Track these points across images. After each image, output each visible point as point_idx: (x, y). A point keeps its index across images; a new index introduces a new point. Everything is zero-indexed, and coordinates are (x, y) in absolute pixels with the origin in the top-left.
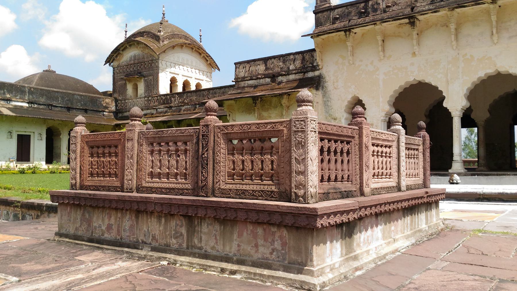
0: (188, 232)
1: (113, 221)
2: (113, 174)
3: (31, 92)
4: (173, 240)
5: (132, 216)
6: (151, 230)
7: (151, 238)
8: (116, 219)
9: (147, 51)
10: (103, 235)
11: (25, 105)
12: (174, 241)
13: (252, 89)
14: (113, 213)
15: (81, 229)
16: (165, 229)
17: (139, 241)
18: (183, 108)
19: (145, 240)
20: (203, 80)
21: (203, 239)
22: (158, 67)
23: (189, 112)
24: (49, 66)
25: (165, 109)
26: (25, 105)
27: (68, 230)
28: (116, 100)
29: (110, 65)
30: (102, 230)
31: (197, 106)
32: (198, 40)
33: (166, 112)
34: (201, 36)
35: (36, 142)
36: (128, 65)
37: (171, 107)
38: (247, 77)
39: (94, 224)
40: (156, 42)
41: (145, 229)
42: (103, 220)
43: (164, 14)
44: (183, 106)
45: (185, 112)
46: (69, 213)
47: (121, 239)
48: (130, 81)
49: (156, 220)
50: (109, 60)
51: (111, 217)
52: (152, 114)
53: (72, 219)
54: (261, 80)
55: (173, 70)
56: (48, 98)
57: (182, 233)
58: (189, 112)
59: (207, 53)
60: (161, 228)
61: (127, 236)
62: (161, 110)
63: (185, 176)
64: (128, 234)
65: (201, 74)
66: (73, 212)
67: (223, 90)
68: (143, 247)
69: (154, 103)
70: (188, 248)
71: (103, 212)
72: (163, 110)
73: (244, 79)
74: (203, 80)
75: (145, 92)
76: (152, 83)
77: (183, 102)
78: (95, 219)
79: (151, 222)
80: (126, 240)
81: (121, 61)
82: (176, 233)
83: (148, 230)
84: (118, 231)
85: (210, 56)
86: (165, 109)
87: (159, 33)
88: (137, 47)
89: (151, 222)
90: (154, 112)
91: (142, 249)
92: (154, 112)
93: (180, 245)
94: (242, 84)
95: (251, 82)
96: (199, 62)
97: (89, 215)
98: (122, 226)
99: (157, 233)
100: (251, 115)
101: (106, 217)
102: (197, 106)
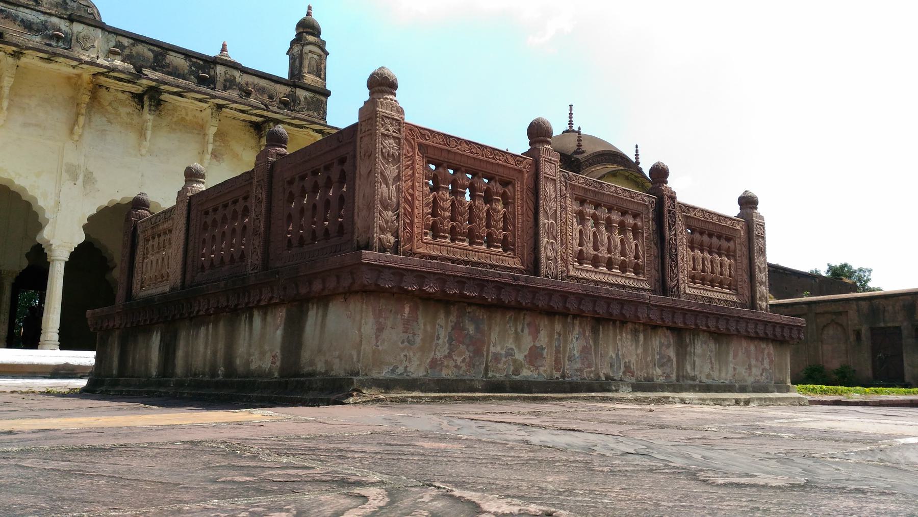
0: (678, 355)
1: (543, 339)
2: (498, 241)
4: (658, 369)
5: (584, 331)
6: (623, 355)
7: (623, 369)
8: (551, 337)
10: (516, 372)
12: (659, 371)
14: (544, 323)
15: (452, 363)
16: (645, 351)
17: (599, 377)
19: (611, 375)
21: (697, 363)
27: (401, 370)
30: (515, 361)
39: (492, 349)
41: (612, 353)
42: (517, 338)
46: (407, 323)
47: (563, 377)
49: (629, 337)
51: (538, 331)
53: (418, 340)
57: (669, 357)
60: (640, 351)
61: (577, 370)
63: (637, 270)
64: (578, 366)
66: (421, 321)
68: (619, 386)
70: (678, 380)
71: (516, 320)
78: (494, 336)
79: (621, 340)
80: (575, 378)
82: (662, 357)
83: (617, 355)
84: (557, 361)
89: (621, 340)
91: (617, 391)
93: (668, 377)
97: (477, 329)
98: (565, 351)
99: (633, 359)
101: (526, 331)
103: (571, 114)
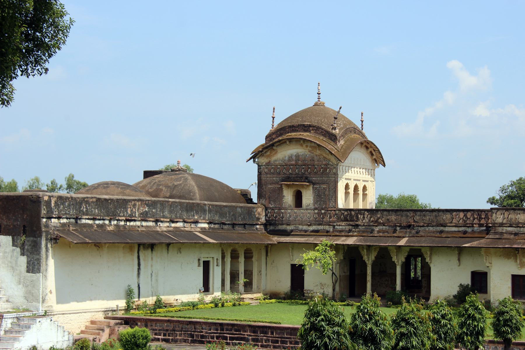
3: (210, 211)
9: (318, 152)
11: (206, 226)
13: (512, 236)
18: (377, 229)
20: (368, 181)
22: (336, 174)
23: (386, 234)
24: (178, 163)
25: (348, 228)
26: (206, 226)
28: (266, 209)
29: (254, 161)
31: (398, 228)
32: (360, 127)
33: (350, 231)
34: (362, 121)
35: (215, 267)
36: (286, 165)
37: (357, 226)
38: (506, 224)
40: (332, 143)
43: (340, 108)
44: (377, 226)
45: (381, 234)
48: (288, 186)
50: (253, 157)
52: (328, 232)
54: (522, 229)
55: (347, 175)
56: (222, 215)
58: (386, 234)
59: (377, 148)
62: (341, 227)
65: (367, 173)
67: (434, 214)
69: (330, 217)
72: (344, 227)
73: (502, 225)
74: (368, 181)
75: (315, 202)
76: (327, 193)
77: (376, 221)
81: (274, 158)
85: (379, 151)
86: (348, 228)
87: (334, 131)
88: (302, 145)
90: (327, 228)
92: (327, 228)
94: (500, 229)
95: (510, 229)
96: (366, 158)
100: (510, 260)
102: (398, 228)
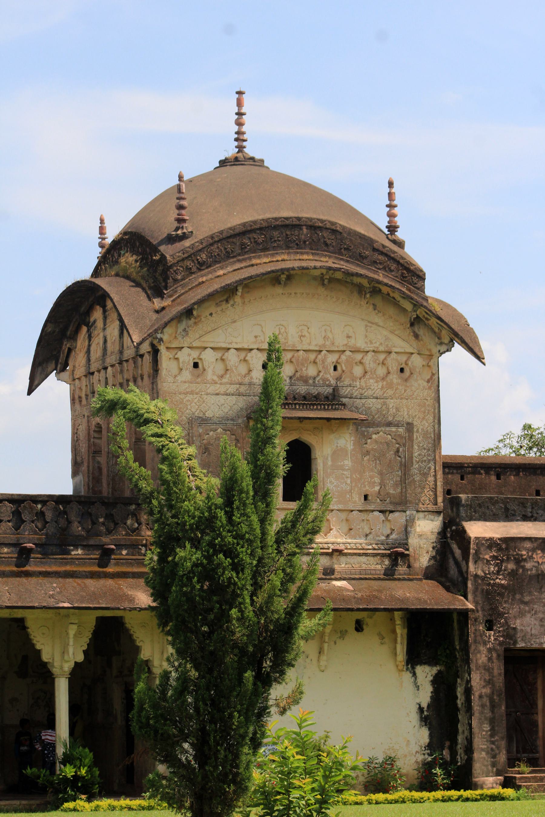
103: (240, 114)
